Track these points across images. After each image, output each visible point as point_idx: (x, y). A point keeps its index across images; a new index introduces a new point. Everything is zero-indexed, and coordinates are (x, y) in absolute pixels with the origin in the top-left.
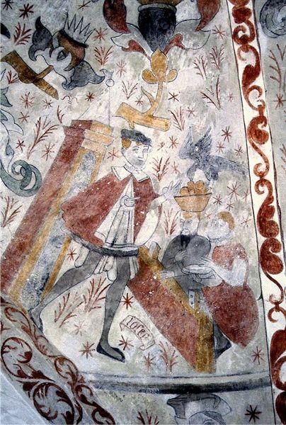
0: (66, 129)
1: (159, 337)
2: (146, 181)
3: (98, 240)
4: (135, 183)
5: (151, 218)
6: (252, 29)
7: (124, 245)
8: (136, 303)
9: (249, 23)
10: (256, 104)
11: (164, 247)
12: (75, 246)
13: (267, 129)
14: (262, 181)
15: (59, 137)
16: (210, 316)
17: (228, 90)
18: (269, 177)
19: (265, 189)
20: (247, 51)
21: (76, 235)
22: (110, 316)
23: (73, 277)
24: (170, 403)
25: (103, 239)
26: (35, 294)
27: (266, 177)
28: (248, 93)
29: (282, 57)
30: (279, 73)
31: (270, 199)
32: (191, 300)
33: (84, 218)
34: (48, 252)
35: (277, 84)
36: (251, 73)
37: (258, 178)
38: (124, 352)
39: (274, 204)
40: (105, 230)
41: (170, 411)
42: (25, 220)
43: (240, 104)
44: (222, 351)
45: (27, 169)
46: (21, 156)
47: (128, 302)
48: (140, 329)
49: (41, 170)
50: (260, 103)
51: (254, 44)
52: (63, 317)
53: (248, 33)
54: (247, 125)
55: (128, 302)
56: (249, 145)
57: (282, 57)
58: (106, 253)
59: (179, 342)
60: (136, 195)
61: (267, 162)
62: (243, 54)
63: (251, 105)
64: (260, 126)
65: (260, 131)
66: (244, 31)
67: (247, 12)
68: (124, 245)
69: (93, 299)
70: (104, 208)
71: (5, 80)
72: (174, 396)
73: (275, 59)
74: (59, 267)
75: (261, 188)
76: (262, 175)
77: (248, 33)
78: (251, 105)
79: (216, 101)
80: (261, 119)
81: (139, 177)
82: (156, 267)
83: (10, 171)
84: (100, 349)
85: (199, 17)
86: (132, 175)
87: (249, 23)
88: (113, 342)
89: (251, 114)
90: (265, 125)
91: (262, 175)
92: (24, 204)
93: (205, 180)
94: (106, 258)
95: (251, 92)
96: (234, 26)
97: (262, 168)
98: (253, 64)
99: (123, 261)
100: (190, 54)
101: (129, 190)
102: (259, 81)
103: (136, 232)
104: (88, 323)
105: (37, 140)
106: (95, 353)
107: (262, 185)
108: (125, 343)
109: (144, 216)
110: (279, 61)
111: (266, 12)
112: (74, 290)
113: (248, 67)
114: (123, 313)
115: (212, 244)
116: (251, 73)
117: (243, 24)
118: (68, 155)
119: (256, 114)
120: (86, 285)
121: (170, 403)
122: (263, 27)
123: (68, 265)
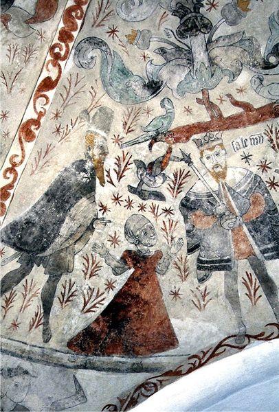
6: (67, 52)
9: (67, 46)
10: (39, 109)
13: (36, 132)
14: (12, 170)
17: (23, 84)
18: (19, 169)
19: (11, 176)
20: (54, 66)
27: (16, 168)
28: (38, 98)
29: (76, 85)
30: (68, 94)
31: (10, 186)
35: (62, 102)
36: (48, 84)
37: (10, 166)
39: (11, 192)
43: (27, 101)
50: (43, 111)
51: (62, 63)
53: (63, 53)
54: (24, 121)
56: (17, 136)
57: (76, 85)
61: (23, 157)
62: (50, 66)
63: (35, 108)
64: (33, 128)
65: (31, 131)
66: (61, 49)
67: (70, 38)
73: (70, 83)
75: (8, 175)
76: (14, 165)
77: (63, 53)
78: (35, 108)
79: (9, 86)
80: (37, 122)
85: (33, 13)
87: (67, 46)
89: (31, 114)
90: (37, 129)
91: (14, 165)
95: (40, 98)
96: (56, 41)
97: (17, 160)
98: (54, 78)
100: (10, 36)
102: (51, 94)
107: (11, 173)
110: (73, 86)
111: (83, 45)
113: (48, 78)
116: (48, 84)
117: (63, 44)
119: (35, 117)
122: (75, 54)
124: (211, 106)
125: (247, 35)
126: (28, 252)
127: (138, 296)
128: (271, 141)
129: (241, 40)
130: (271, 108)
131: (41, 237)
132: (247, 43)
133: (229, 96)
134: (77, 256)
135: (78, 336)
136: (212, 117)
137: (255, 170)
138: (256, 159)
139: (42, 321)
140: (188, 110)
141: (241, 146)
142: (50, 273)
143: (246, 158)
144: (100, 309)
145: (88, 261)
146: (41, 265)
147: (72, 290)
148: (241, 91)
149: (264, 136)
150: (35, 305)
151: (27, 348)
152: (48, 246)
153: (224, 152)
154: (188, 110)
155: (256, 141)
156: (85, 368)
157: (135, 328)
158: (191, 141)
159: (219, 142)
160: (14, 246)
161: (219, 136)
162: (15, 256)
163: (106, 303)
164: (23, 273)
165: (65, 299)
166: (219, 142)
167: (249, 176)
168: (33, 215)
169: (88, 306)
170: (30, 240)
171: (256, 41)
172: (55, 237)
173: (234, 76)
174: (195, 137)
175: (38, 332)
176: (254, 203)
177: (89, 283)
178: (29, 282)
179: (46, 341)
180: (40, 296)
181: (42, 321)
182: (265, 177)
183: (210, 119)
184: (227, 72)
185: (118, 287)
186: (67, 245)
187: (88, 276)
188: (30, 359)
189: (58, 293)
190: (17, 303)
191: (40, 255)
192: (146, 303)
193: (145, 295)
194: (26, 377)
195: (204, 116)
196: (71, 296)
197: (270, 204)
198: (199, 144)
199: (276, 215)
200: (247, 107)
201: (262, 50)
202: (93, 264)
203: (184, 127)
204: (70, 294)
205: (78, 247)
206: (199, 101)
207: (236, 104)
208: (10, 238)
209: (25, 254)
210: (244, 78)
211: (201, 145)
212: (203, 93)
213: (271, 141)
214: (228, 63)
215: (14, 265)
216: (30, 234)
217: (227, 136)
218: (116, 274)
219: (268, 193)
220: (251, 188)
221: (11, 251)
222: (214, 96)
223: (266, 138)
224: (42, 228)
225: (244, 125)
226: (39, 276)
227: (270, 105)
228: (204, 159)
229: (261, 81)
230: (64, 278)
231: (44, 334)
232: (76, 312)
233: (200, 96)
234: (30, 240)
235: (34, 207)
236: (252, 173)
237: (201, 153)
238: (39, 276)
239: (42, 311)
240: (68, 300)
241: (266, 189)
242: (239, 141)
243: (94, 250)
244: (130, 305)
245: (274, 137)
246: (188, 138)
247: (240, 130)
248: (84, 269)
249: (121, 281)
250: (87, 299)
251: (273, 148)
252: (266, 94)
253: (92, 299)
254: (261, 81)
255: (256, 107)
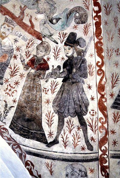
124: (22, 13)
125: (55, 6)
128: (29, 44)
129: (52, 5)
130: (39, 34)
132: (53, 8)
133: (31, 17)
136: (19, 17)
137: (14, 47)
138: (18, 44)
140: (14, 6)
141: (18, 35)
143: (16, 41)
148: (36, 19)
149: (28, 40)
153: (11, 31)
154: (14, 6)
155: (24, 39)
158: (4, 16)
159: (13, 27)
161: (15, 25)
166: (13, 27)
167: (10, 47)
171: (56, 10)
173: (39, 12)
174: (7, 17)
176: (3, 56)
182: (15, 52)
183: (18, 16)
184: (38, 9)
195: (17, 14)
197: (8, 62)
198: (6, 20)
199: (6, 67)
200: (33, 26)
201: (55, 15)
203: (7, 9)
206: (21, 7)
207: (31, 21)
210: (41, 17)
211: (7, 21)
212: (25, 7)
213: (29, 44)
214: (42, 7)
217: (17, 28)
219: (11, 58)
220: (7, 51)
222: (27, 11)
223: (28, 41)
225: (26, 30)
227: (40, 33)
228: (3, 27)
229: (45, 23)
233: (23, 6)
236: (12, 47)
237: (4, 24)
241: (12, 56)
242: (19, 34)
245: (30, 43)
246: (5, 14)
247: (23, 30)
251: (27, 47)
252: (42, 29)
254: (45, 23)
255: (35, 29)
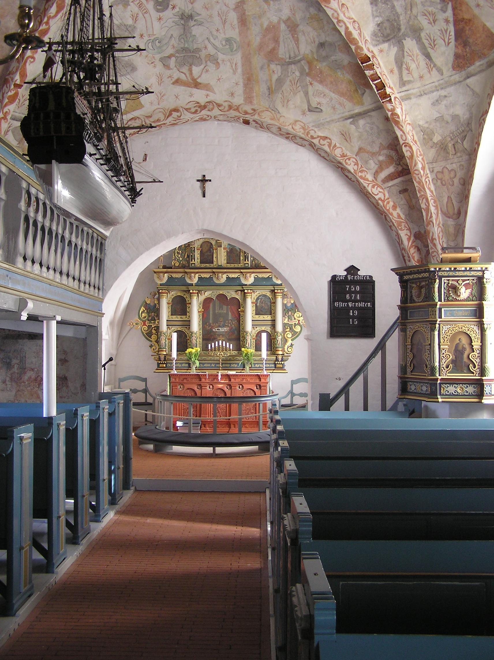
0: (234, 10)
1: (333, 95)
2: (289, 19)
3: (282, 59)
4: (285, 22)
5: (302, 39)
7: (295, 57)
8: (315, 84)
11: (314, 50)
12: (273, 66)
15: (233, 17)
16: (351, 79)
21: (271, 61)
22: (306, 94)
23: (280, 81)
24: (351, 123)
25: (284, 57)
26: (267, 98)
32: (339, 73)
33: (269, 50)
34: (263, 76)
37: (337, 20)
38: (320, 107)
40: (282, 52)
41: (353, 127)
42: (242, 66)
44: (364, 94)
45: (228, 41)
46: (221, 36)
47: (311, 84)
48: (323, 94)
49: (235, 37)
52: (285, 103)
55: (311, 84)
58: (290, 63)
59: (342, 94)
60: (288, 28)
68: (295, 57)
69: (295, 89)
70: (276, 40)
71: (189, 4)
72: (351, 120)
74: (271, 81)
75: (340, 24)
81: (284, 18)
82: (316, 62)
83: (221, 46)
84: (310, 110)
86: (280, 18)
88: (314, 105)
92: (238, 58)
93: (316, 12)
94: (290, 66)
99: (299, 65)
101: (283, 26)
103: (298, 47)
104: (299, 99)
105: (224, 22)
106: (308, 113)
108: (319, 103)
109: (298, 37)
112: (284, 88)
114: (310, 90)
115: (336, 44)
118: (243, 21)
120: (288, 82)
121: (351, 123)
123: (275, 77)
126: (394, 38)
127: (463, 19)
131: (393, 25)
134: (419, 18)
135: (454, 61)
139: (432, 66)
142: (414, 38)
144: (453, 37)
145: (426, 15)
146: (406, 38)
147: (432, 38)
150: (422, 60)
151: (437, 84)
152: (400, 26)
156: (468, 77)
157: (475, 40)
160: (384, 42)
162: (390, 46)
163: (453, 33)
164: (402, 48)
165: (433, 46)
168: (377, 19)
169: (447, 40)
170: (388, 31)
172: (399, 18)
175: (434, 72)
177: (436, 27)
178: (408, 51)
179: (442, 74)
180: (420, 53)
181: (432, 66)
185: (451, 19)
186: (408, 16)
187: (433, 24)
188: (442, 89)
189: (427, 45)
190: (413, 66)
191: (401, 34)
192: (470, 20)
193: (467, 16)
194: (446, 99)
196: (434, 42)
202: (430, 14)
204: (433, 41)
205: (415, 11)
208: (378, 41)
209: (393, 40)
215: (394, 50)
216: (385, 29)
218: (445, 12)
221: (385, 46)
224: (388, 20)
226: (410, 44)
230: (423, 35)
231: (438, 71)
232: (443, 48)
234: (388, 31)
235: (373, 15)
238: (410, 44)
239: (428, 60)
240: (435, 45)
243: (424, 6)
244: (464, 27)
248: (428, 21)
249: (449, 13)
250: (443, 37)
253: (445, 36)
